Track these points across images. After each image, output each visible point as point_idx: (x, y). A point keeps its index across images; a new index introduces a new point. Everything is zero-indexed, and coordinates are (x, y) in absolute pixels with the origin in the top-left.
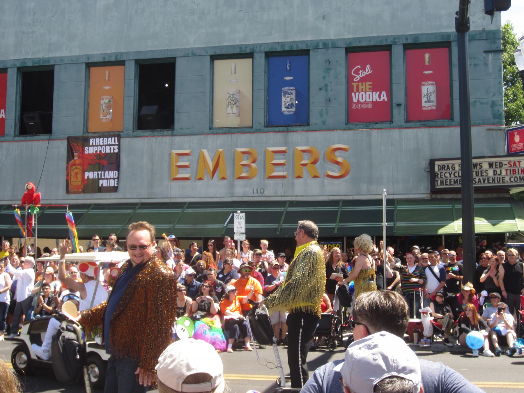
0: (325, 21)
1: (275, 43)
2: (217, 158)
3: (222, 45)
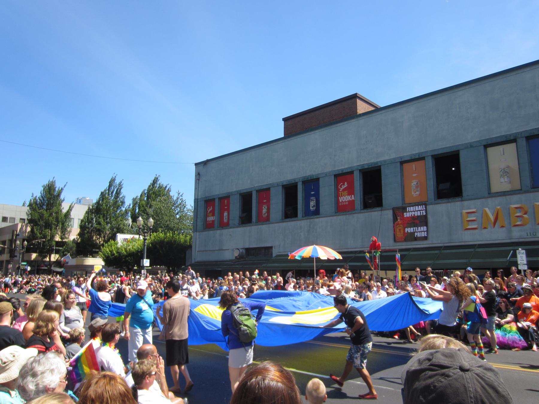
3: (354, 165)
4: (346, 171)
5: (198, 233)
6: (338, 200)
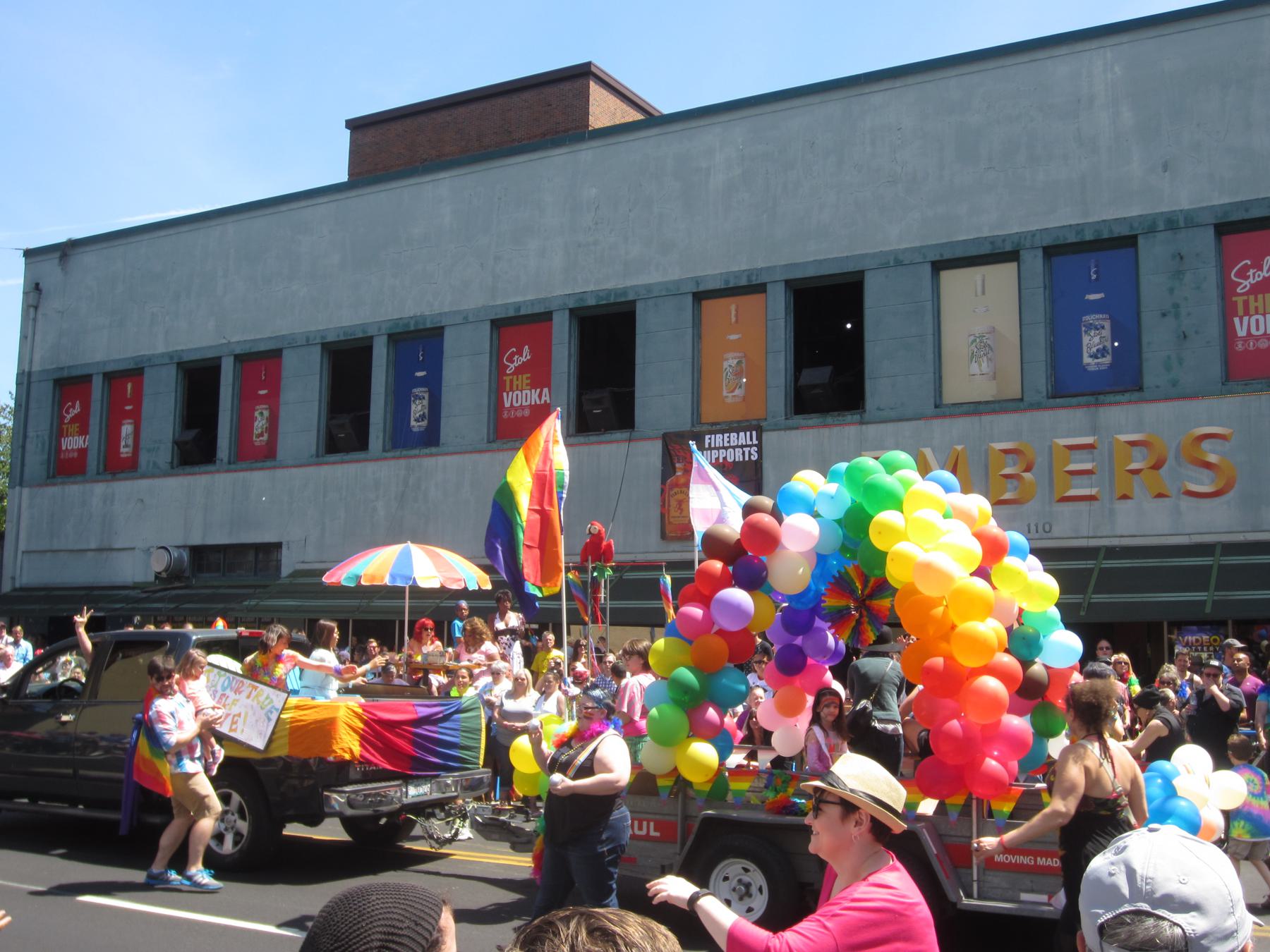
0: (1167, 174)
1: (1064, 226)
2: (953, 462)
4: (529, 312)
5: (26, 491)
6: (500, 401)
